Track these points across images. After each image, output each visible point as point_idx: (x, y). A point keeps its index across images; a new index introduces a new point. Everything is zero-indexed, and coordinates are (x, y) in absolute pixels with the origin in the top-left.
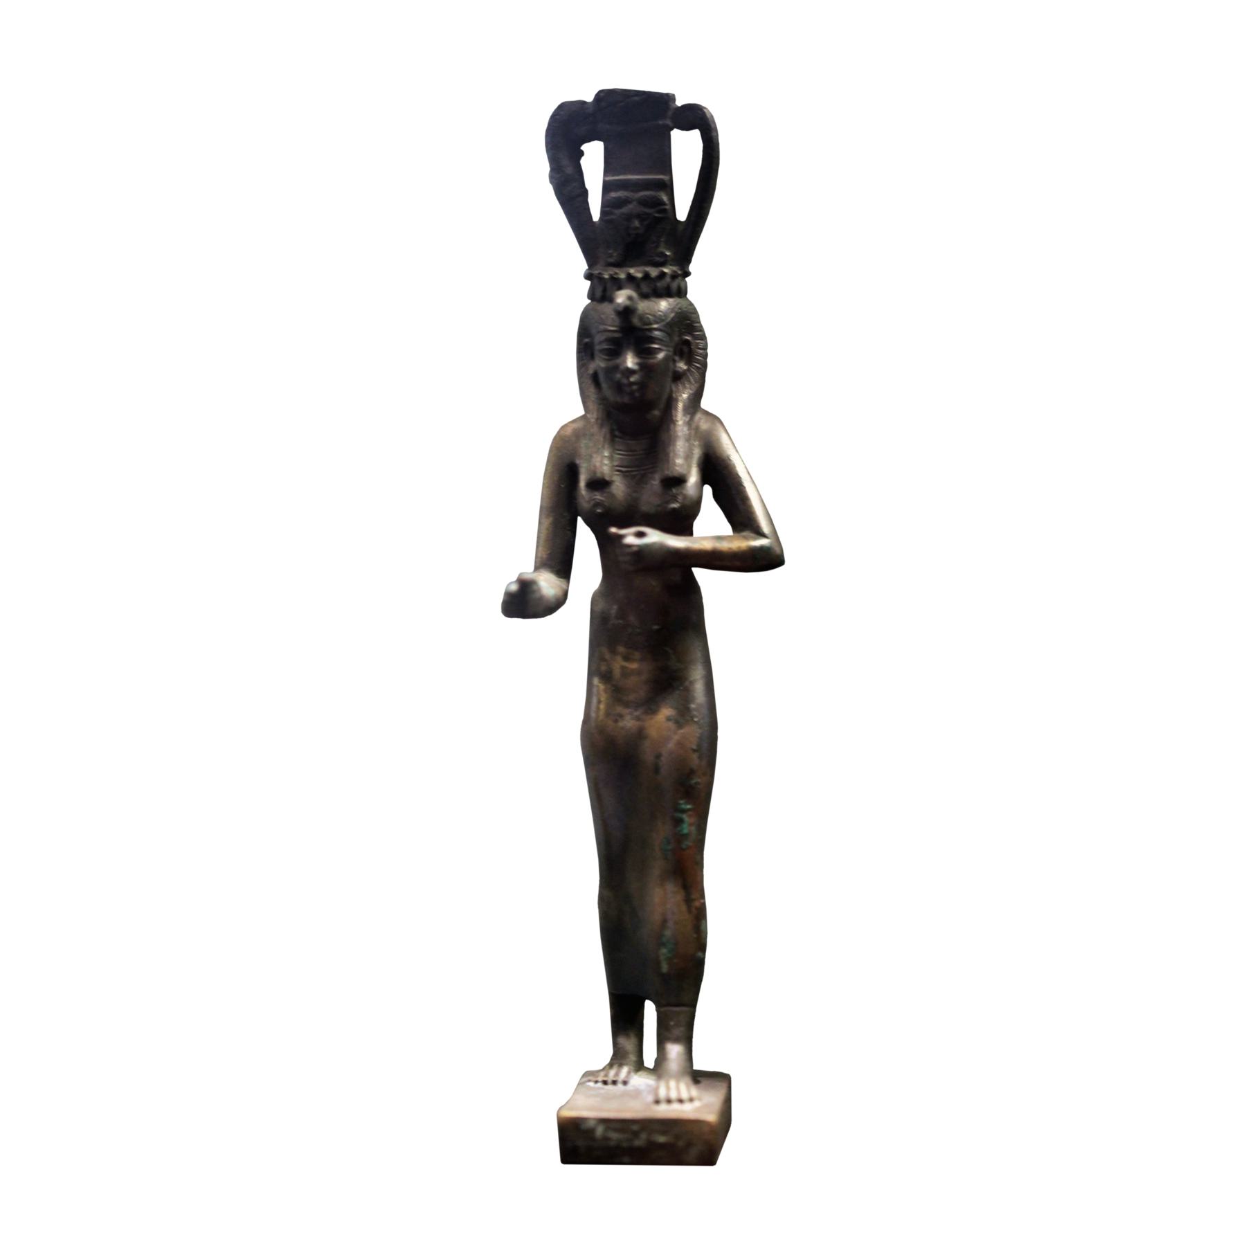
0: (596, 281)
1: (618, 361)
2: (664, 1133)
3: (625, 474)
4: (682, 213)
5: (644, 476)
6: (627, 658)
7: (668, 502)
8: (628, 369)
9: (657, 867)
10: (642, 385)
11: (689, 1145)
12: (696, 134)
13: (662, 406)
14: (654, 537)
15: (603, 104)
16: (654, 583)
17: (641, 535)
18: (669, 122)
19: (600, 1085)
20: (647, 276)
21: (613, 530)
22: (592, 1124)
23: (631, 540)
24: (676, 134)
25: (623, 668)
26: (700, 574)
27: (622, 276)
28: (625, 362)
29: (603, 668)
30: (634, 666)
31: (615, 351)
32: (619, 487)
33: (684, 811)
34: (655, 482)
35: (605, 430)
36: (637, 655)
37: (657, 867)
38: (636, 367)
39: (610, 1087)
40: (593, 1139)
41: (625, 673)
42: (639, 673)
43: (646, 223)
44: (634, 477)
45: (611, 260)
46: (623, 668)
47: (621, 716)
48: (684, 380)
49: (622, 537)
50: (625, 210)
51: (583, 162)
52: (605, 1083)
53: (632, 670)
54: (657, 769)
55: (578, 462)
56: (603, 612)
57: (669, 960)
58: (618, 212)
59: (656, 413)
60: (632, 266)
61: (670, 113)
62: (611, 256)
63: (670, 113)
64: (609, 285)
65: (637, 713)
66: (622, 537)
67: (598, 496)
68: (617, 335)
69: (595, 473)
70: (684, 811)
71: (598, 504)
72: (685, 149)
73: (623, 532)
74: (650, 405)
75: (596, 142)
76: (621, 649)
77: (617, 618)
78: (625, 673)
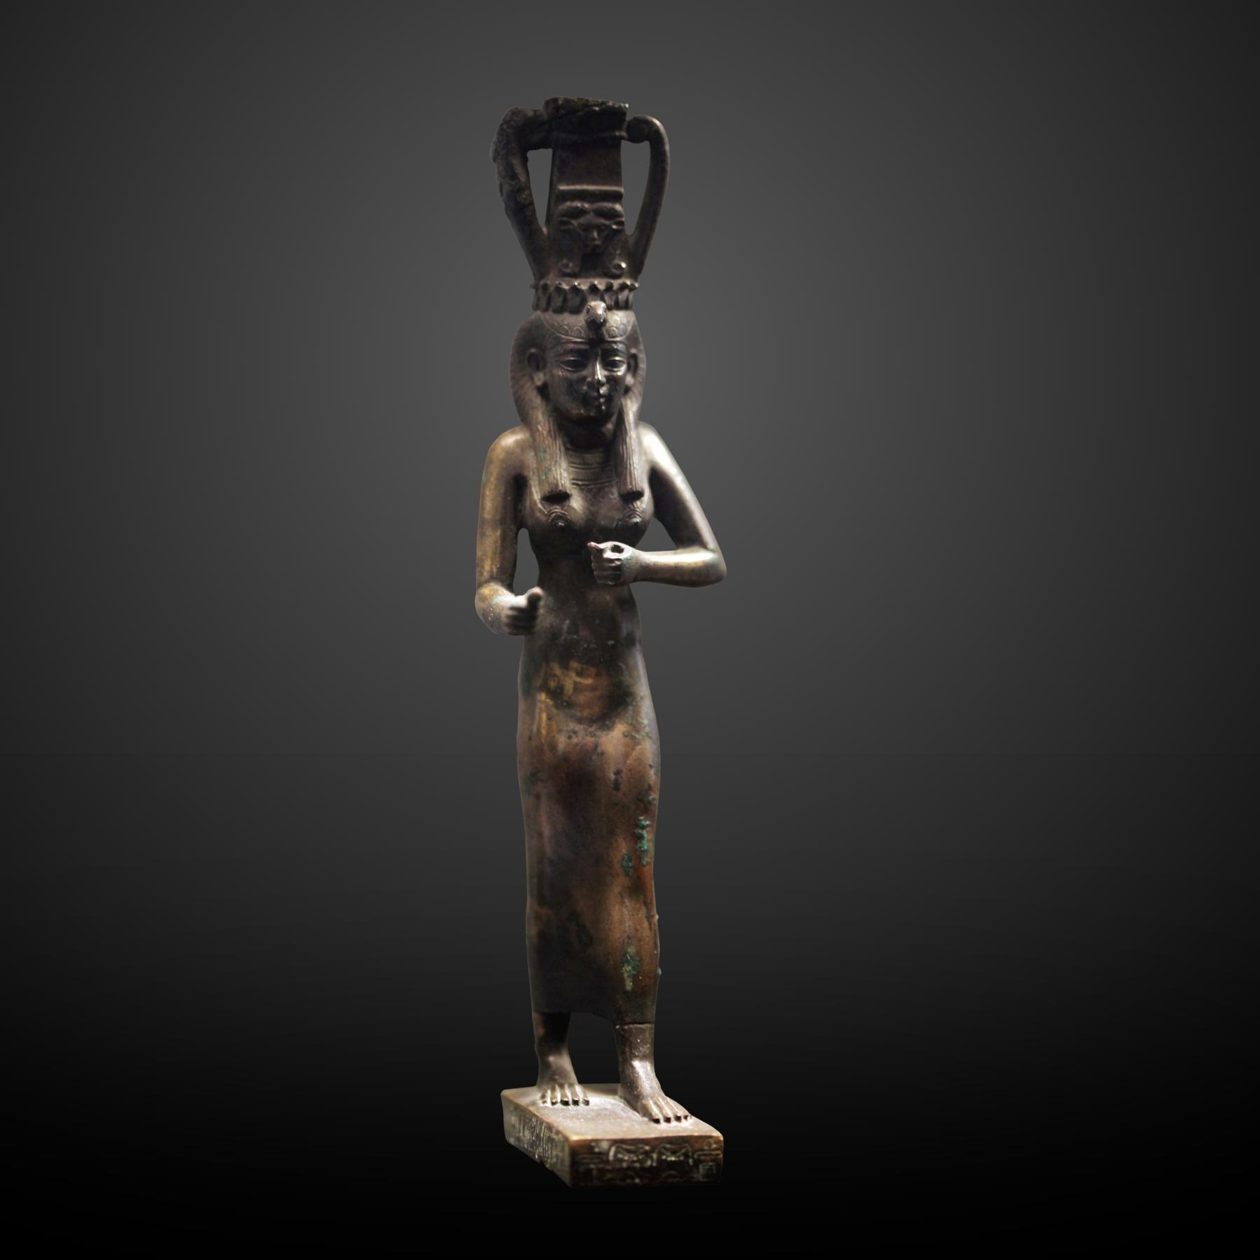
0: (540, 291)
1: (585, 373)
2: (674, 1153)
3: (581, 488)
4: (630, 228)
5: (600, 490)
6: (580, 674)
7: (630, 517)
8: (599, 381)
9: (619, 884)
10: (609, 398)
11: (697, 1162)
12: (646, 144)
13: (614, 418)
14: (629, 552)
15: (562, 112)
16: (608, 598)
17: (617, 549)
18: (624, 134)
19: (559, 1106)
20: (609, 288)
21: (593, 544)
22: (605, 1145)
23: (609, 555)
24: (625, 145)
25: (575, 683)
26: (637, 589)
27: (584, 287)
28: (594, 373)
29: (552, 684)
30: (589, 681)
31: (582, 359)
32: (577, 503)
33: (643, 828)
34: (614, 495)
35: (559, 442)
36: (593, 670)
37: (619, 884)
38: (604, 380)
39: (571, 1107)
40: (608, 1162)
41: (577, 688)
42: (593, 688)
43: (604, 234)
44: (590, 491)
45: (568, 271)
46: (575, 683)
47: (575, 733)
48: (630, 394)
49: (601, 551)
50: (582, 220)
51: (529, 164)
52: (566, 1103)
53: (587, 686)
54: (617, 785)
55: (526, 473)
56: (552, 627)
57: (635, 978)
58: (575, 222)
59: (610, 426)
60: (594, 277)
61: (625, 126)
62: (567, 266)
63: (625, 126)
64: (569, 296)
65: (592, 729)
66: (601, 551)
67: (557, 509)
68: (583, 347)
69: (557, 485)
70: (643, 828)
71: (559, 517)
72: (635, 157)
73: (602, 546)
74: (606, 417)
75: (541, 150)
76: (574, 664)
77: (569, 632)
78: (577, 688)
